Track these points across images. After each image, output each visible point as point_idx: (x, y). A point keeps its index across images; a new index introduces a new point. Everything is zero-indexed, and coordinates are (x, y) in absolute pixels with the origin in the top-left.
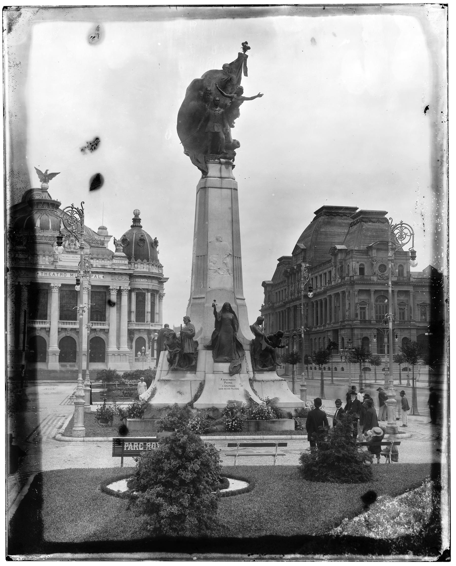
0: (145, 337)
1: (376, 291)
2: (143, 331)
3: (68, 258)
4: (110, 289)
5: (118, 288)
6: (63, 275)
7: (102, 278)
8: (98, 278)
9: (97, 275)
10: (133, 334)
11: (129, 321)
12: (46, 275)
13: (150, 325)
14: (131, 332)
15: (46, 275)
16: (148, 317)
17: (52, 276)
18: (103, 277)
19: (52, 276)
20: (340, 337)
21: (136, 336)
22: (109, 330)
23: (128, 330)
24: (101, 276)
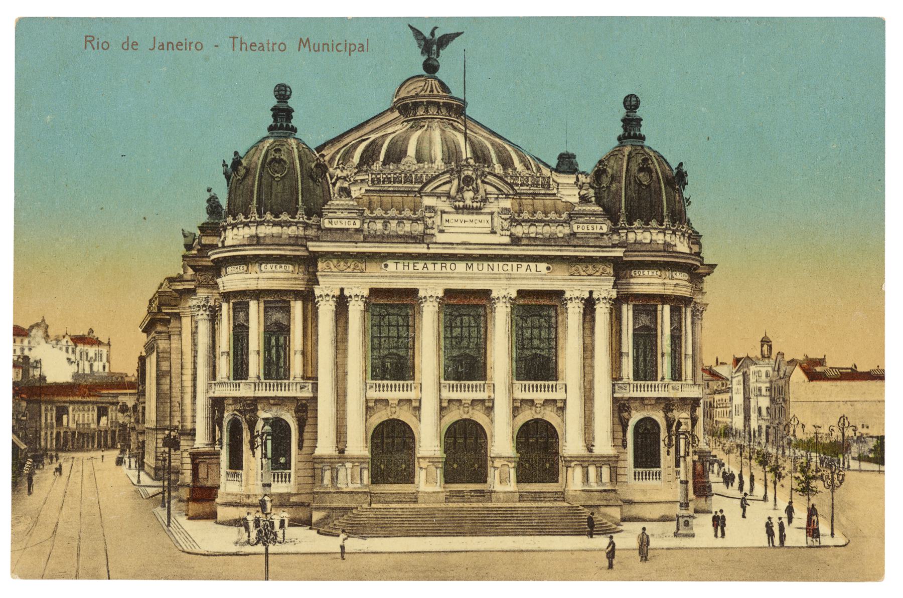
0: (658, 416)
2: (653, 402)
4: (565, 300)
5: (586, 295)
7: (545, 271)
9: (532, 265)
10: (628, 410)
11: (616, 378)
12: (406, 268)
13: (670, 386)
14: (621, 407)
15: (406, 268)
16: (664, 367)
17: (420, 270)
18: (548, 269)
19: (420, 271)
21: (635, 417)
22: (565, 401)
23: (615, 400)
24: (542, 266)
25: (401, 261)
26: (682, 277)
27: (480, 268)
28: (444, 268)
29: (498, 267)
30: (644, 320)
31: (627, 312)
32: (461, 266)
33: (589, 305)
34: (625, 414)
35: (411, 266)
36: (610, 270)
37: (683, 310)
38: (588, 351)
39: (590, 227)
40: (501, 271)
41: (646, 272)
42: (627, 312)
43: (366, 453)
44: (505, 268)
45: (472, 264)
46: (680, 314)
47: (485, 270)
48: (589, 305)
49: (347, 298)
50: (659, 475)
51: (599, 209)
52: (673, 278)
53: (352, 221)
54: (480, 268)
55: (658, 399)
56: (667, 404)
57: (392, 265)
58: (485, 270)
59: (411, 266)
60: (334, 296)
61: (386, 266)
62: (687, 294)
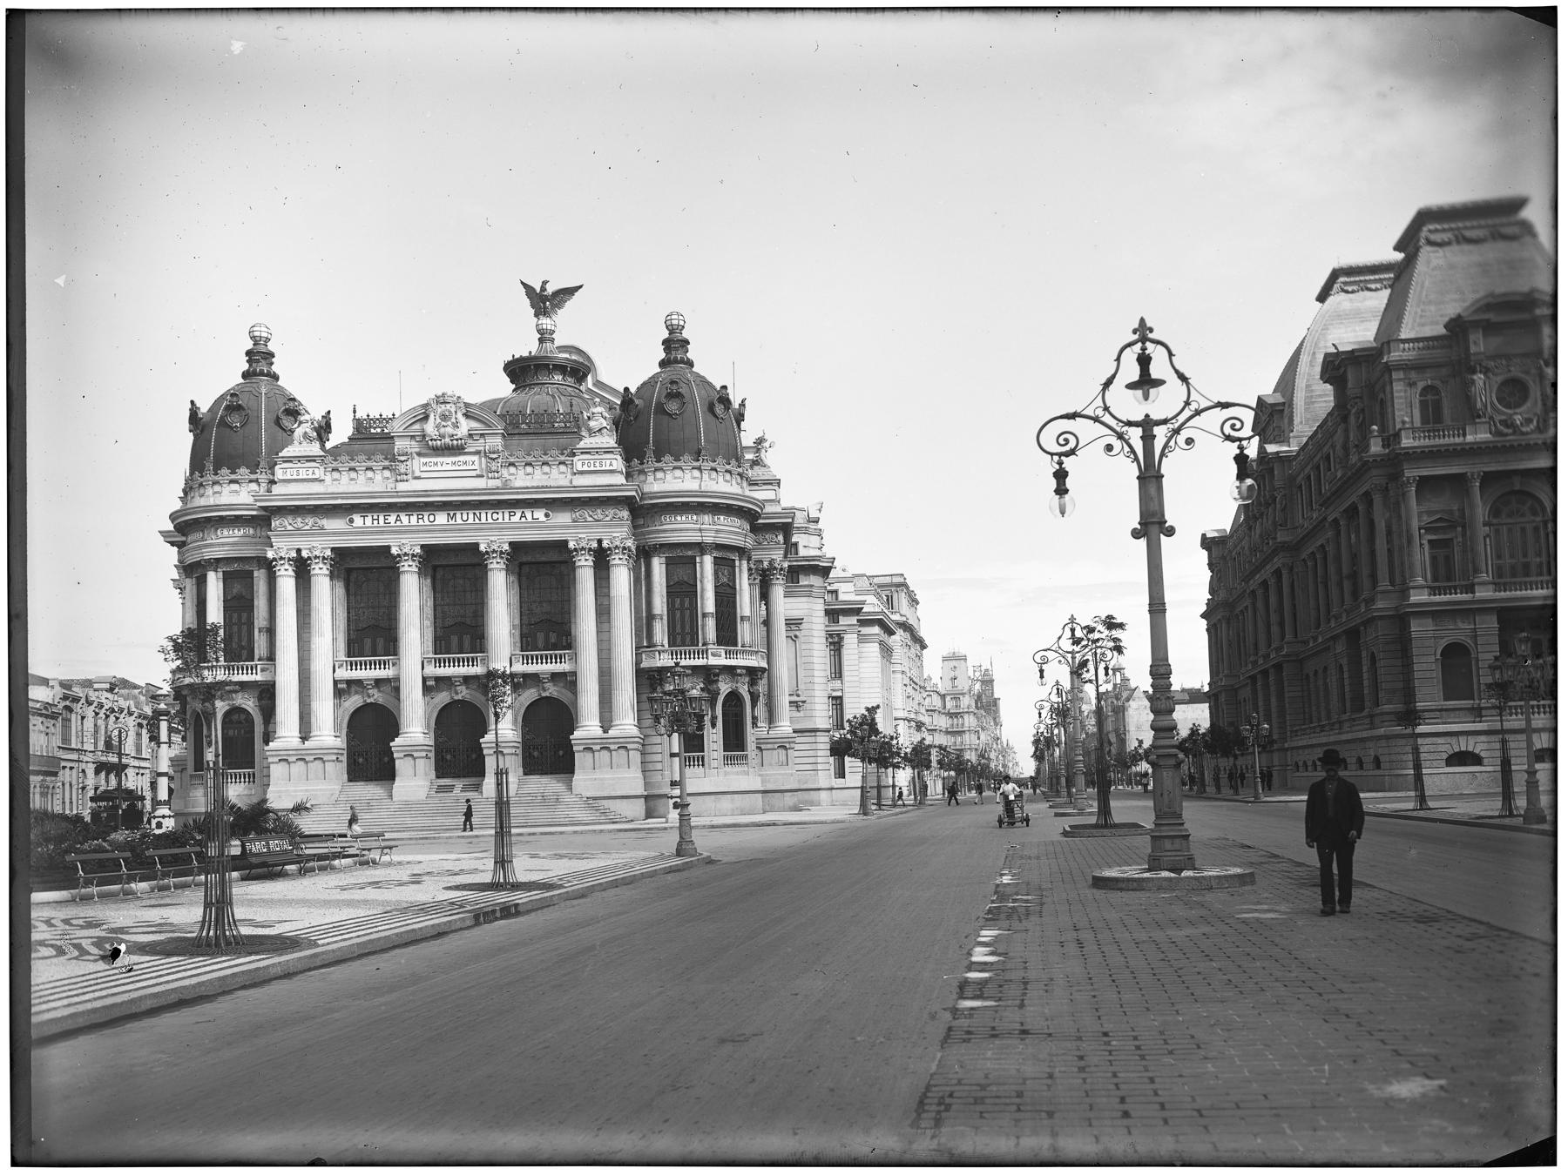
1: (1488, 479)
3: (439, 468)
6: (426, 518)
8: (530, 519)
12: (375, 522)
14: (648, 680)
18: (547, 515)
19: (393, 524)
20: (1364, 654)
25: (370, 515)
27: (465, 518)
28: (421, 521)
29: (486, 516)
31: (658, 566)
32: (441, 518)
33: (602, 559)
35: (381, 518)
36: (625, 514)
37: (737, 563)
38: (604, 612)
39: (597, 464)
40: (490, 520)
41: (679, 518)
42: (658, 566)
43: (341, 743)
44: (495, 516)
45: (455, 514)
46: (734, 567)
47: (471, 521)
48: (602, 559)
50: (703, 761)
52: (714, 523)
53: (311, 470)
54: (465, 518)
55: (694, 668)
56: (709, 675)
57: (358, 520)
58: (471, 521)
59: (381, 518)
60: (289, 560)
61: (351, 521)
62: (740, 544)
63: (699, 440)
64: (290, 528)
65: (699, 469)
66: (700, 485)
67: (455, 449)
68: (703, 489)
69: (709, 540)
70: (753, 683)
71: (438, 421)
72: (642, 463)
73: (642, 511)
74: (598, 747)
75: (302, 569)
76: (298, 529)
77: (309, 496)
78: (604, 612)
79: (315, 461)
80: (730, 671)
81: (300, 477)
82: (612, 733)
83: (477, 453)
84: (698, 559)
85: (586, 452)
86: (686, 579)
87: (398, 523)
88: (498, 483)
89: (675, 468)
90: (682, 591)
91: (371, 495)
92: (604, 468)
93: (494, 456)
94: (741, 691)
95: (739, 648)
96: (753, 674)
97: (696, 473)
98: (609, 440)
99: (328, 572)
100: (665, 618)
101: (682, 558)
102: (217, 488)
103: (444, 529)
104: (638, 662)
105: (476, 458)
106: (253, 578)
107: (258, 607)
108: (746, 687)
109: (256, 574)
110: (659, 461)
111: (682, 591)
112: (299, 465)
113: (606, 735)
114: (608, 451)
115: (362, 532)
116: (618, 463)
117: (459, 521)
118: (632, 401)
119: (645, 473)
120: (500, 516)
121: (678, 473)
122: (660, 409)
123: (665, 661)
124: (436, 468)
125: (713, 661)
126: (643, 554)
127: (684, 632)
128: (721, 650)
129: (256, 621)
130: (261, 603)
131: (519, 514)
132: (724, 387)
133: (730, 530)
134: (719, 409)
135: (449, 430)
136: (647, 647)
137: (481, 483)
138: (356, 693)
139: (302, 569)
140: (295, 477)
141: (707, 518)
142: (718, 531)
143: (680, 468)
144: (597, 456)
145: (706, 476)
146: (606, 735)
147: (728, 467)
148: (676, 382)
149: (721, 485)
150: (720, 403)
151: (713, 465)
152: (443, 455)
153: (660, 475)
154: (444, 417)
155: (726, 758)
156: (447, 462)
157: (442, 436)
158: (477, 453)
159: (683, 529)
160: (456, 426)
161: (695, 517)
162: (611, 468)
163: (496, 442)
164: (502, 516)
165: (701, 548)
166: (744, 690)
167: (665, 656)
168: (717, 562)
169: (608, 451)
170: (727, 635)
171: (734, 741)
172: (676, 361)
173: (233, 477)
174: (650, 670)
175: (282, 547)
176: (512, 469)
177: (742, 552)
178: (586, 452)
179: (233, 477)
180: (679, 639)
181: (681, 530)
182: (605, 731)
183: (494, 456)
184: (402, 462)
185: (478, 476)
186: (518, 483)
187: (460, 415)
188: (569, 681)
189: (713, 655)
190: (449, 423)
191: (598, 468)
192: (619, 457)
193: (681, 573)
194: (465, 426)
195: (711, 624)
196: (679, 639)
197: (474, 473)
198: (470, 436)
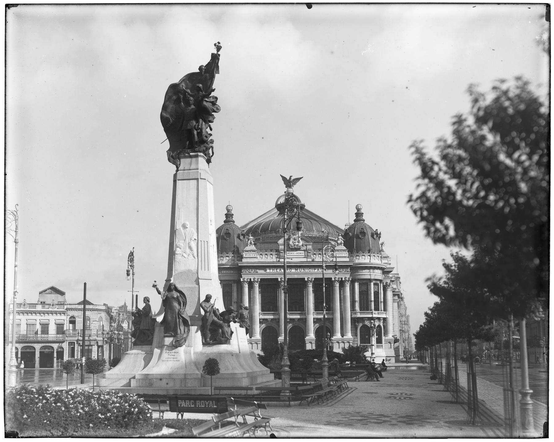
14: (355, 321)
26: (379, 272)
29: (307, 270)
30: (364, 288)
31: (357, 285)
32: (293, 271)
33: (342, 284)
34: (357, 324)
38: (342, 300)
40: (308, 271)
41: (363, 271)
42: (357, 285)
44: (310, 270)
49: (252, 282)
51: (345, 248)
52: (374, 272)
57: (268, 271)
61: (266, 270)
63: (369, 246)
64: (247, 272)
65: (370, 256)
66: (370, 261)
67: (298, 249)
68: (371, 262)
69: (372, 278)
70: (384, 322)
71: (293, 240)
72: (352, 253)
73: (355, 269)
74: (341, 342)
75: (251, 284)
76: (250, 273)
77: (251, 263)
78: (342, 300)
79: (255, 252)
80: (379, 319)
81: (251, 256)
82: (345, 337)
83: (304, 250)
84: (369, 284)
85: (338, 250)
86: (365, 290)
87: (280, 271)
88: (310, 260)
89: (363, 255)
90: (364, 294)
91: (273, 262)
92: (343, 256)
93: (310, 251)
94: (381, 325)
95: (380, 312)
96: (385, 319)
97: (369, 257)
98: (343, 247)
99: (258, 286)
100: (359, 302)
101: (365, 284)
102: (222, 258)
103: (293, 274)
104: (351, 316)
105: (304, 252)
106: (232, 286)
107: (234, 295)
108: (382, 324)
109: (233, 285)
110: (357, 253)
111: (364, 294)
112: (250, 253)
113: (343, 338)
114: (344, 250)
115: (270, 274)
116: (346, 254)
117: (299, 271)
118: (348, 234)
119: (353, 257)
120: (311, 270)
121: (363, 257)
122: (358, 237)
123: (359, 315)
124: (291, 255)
125: (374, 316)
126: (353, 282)
127: (365, 307)
128: (377, 312)
129: (233, 300)
130: (235, 295)
131: (317, 270)
132: (377, 230)
133: (377, 274)
134: (375, 236)
135: (297, 243)
136: (353, 311)
137: (305, 260)
138: (265, 323)
139: (251, 284)
140: (249, 256)
141: (371, 270)
142: (375, 275)
143: (364, 255)
144: (340, 252)
145: (372, 257)
146: (343, 338)
147: (378, 255)
148: (363, 229)
149: (375, 261)
150: (376, 235)
151: (374, 254)
152: (294, 251)
153: (358, 257)
154: (295, 239)
155: (377, 346)
156: (295, 253)
157: (295, 245)
158: (304, 250)
159: (366, 274)
160: (299, 242)
161: (368, 271)
162: (345, 256)
163: (310, 247)
164: (312, 271)
165: (370, 280)
166: (382, 325)
167: (359, 314)
168: (375, 284)
169: (344, 250)
170: (377, 309)
171: (379, 341)
172: (360, 220)
173: (227, 255)
174: (355, 318)
175: (246, 276)
176: (315, 256)
177: (381, 281)
178: (338, 250)
179: (227, 255)
180: (363, 309)
181: (364, 275)
182: (343, 337)
183: (310, 251)
184: (281, 252)
185: (304, 257)
186: (317, 260)
187: (300, 239)
188: (331, 321)
189: (374, 314)
190: (296, 241)
191: (341, 256)
192: (347, 253)
193: (364, 288)
194: (301, 243)
195: (373, 303)
196: (363, 309)
197: (303, 257)
198: (302, 245)
